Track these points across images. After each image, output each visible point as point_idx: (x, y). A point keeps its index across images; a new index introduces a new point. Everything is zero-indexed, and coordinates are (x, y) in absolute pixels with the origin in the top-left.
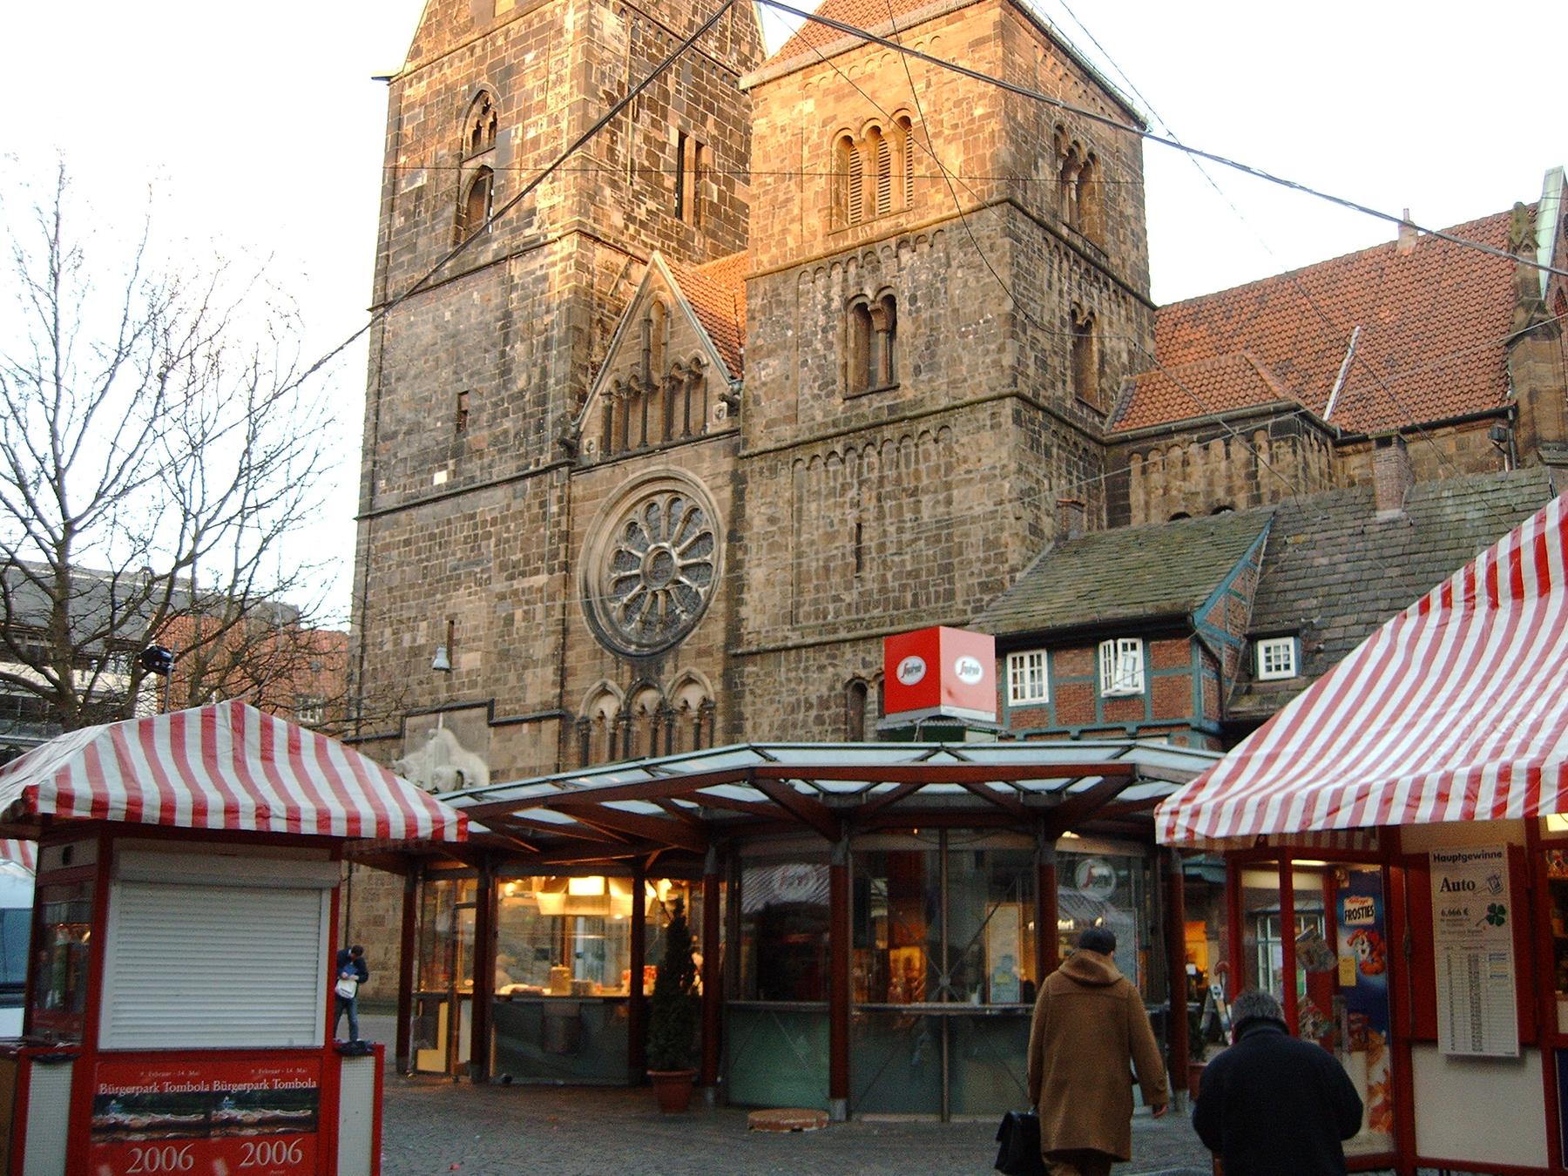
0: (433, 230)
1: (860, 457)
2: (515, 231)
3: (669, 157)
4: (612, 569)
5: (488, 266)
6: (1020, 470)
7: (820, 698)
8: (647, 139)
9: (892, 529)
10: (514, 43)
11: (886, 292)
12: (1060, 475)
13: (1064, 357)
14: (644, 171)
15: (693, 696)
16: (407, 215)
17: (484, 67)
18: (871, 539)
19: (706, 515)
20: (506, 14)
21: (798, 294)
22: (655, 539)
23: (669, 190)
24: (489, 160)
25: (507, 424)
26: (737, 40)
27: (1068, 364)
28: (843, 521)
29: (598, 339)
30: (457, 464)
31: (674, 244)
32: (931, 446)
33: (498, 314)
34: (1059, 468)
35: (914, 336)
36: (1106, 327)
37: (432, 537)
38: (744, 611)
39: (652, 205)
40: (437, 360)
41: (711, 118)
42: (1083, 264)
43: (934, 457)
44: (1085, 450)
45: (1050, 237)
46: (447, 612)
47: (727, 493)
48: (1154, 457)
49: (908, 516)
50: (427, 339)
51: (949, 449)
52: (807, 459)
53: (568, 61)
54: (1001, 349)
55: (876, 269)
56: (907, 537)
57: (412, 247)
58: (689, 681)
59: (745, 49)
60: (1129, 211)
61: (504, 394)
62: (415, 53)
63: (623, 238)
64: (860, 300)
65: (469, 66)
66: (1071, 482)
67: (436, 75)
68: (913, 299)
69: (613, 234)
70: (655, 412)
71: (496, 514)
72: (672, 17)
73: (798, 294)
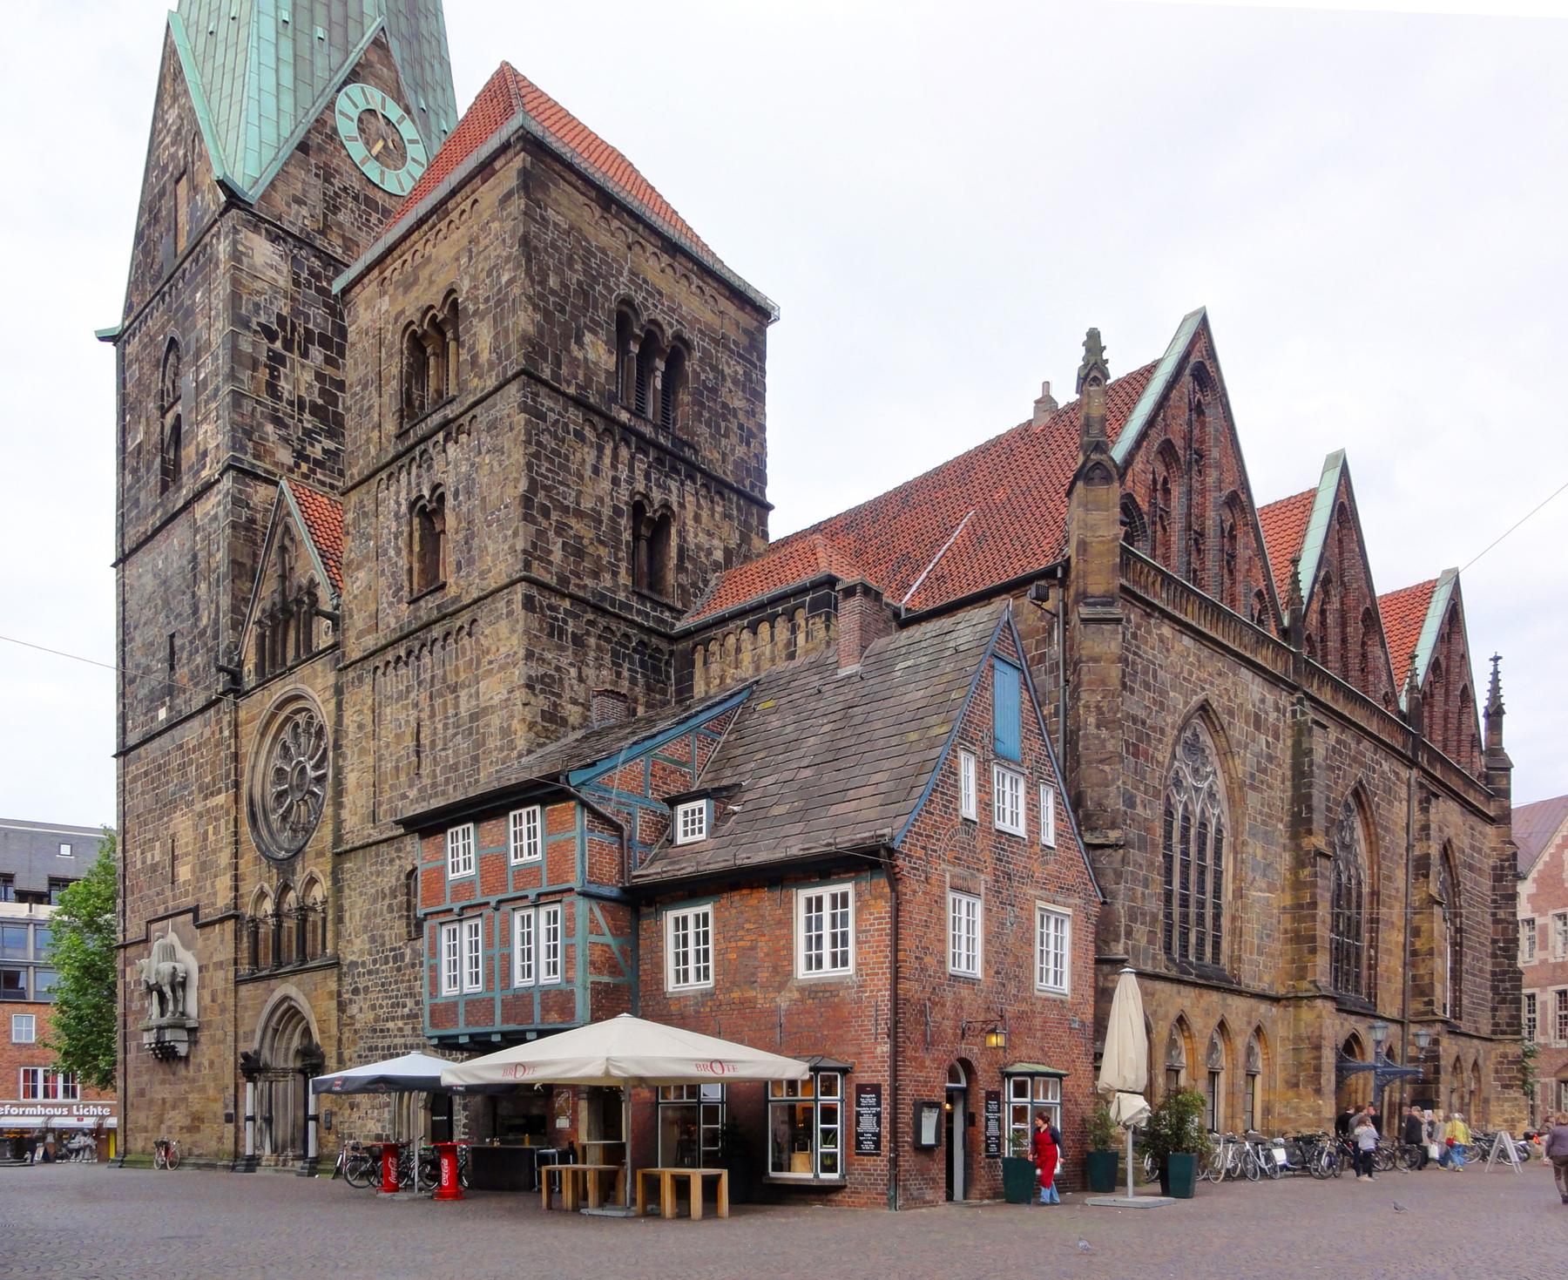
4: (274, 784)
6: (529, 655)
9: (440, 726)
13: (617, 548)
28: (407, 722)
42: (652, 454)
49: (451, 712)
51: (478, 641)
54: (515, 534)
56: (451, 731)
60: (738, 403)
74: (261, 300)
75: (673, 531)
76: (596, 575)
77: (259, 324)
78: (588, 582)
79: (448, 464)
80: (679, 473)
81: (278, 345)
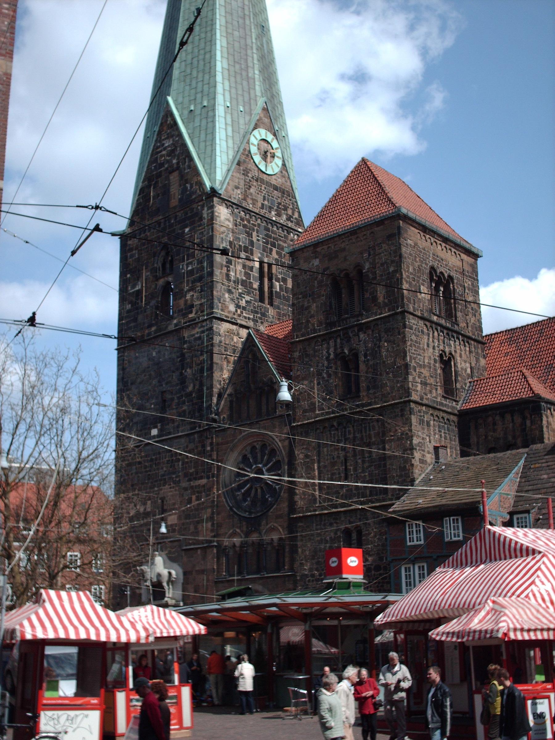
0: (145, 312)
1: (345, 428)
2: (185, 315)
3: (255, 273)
5: (172, 331)
7: (331, 538)
8: (244, 266)
9: (360, 461)
11: (354, 352)
12: (435, 434)
14: (244, 283)
15: (275, 537)
16: (131, 302)
18: (351, 465)
20: (175, 207)
21: (315, 351)
22: (256, 463)
23: (255, 289)
24: (170, 279)
25: (185, 408)
26: (286, 209)
27: (438, 380)
28: (338, 457)
29: (225, 366)
30: (162, 426)
31: (259, 315)
33: (178, 354)
34: (434, 430)
35: (367, 373)
36: (459, 358)
37: (152, 460)
38: (297, 498)
39: (248, 298)
40: (150, 375)
41: (274, 250)
42: (445, 331)
43: (377, 428)
44: (448, 420)
45: (427, 323)
46: (160, 496)
47: (286, 443)
51: (383, 424)
52: (321, 428)
53: (205, 233)
55: (349, 340)
56: (367, 464)
57: (135, 320)
58: (273, 529)
59: (290, 212)
61: (183, 393)
62: (132, 223)
63: (235, 317)
66: (441, 435)
68: (365, 356)
69: (230, 315)
72: (254, 204)
73: (315, 351)
74: (223, 236)
75: (453, 363)
76: (431, 392)
78: (429, 396)
79: (360, 341)
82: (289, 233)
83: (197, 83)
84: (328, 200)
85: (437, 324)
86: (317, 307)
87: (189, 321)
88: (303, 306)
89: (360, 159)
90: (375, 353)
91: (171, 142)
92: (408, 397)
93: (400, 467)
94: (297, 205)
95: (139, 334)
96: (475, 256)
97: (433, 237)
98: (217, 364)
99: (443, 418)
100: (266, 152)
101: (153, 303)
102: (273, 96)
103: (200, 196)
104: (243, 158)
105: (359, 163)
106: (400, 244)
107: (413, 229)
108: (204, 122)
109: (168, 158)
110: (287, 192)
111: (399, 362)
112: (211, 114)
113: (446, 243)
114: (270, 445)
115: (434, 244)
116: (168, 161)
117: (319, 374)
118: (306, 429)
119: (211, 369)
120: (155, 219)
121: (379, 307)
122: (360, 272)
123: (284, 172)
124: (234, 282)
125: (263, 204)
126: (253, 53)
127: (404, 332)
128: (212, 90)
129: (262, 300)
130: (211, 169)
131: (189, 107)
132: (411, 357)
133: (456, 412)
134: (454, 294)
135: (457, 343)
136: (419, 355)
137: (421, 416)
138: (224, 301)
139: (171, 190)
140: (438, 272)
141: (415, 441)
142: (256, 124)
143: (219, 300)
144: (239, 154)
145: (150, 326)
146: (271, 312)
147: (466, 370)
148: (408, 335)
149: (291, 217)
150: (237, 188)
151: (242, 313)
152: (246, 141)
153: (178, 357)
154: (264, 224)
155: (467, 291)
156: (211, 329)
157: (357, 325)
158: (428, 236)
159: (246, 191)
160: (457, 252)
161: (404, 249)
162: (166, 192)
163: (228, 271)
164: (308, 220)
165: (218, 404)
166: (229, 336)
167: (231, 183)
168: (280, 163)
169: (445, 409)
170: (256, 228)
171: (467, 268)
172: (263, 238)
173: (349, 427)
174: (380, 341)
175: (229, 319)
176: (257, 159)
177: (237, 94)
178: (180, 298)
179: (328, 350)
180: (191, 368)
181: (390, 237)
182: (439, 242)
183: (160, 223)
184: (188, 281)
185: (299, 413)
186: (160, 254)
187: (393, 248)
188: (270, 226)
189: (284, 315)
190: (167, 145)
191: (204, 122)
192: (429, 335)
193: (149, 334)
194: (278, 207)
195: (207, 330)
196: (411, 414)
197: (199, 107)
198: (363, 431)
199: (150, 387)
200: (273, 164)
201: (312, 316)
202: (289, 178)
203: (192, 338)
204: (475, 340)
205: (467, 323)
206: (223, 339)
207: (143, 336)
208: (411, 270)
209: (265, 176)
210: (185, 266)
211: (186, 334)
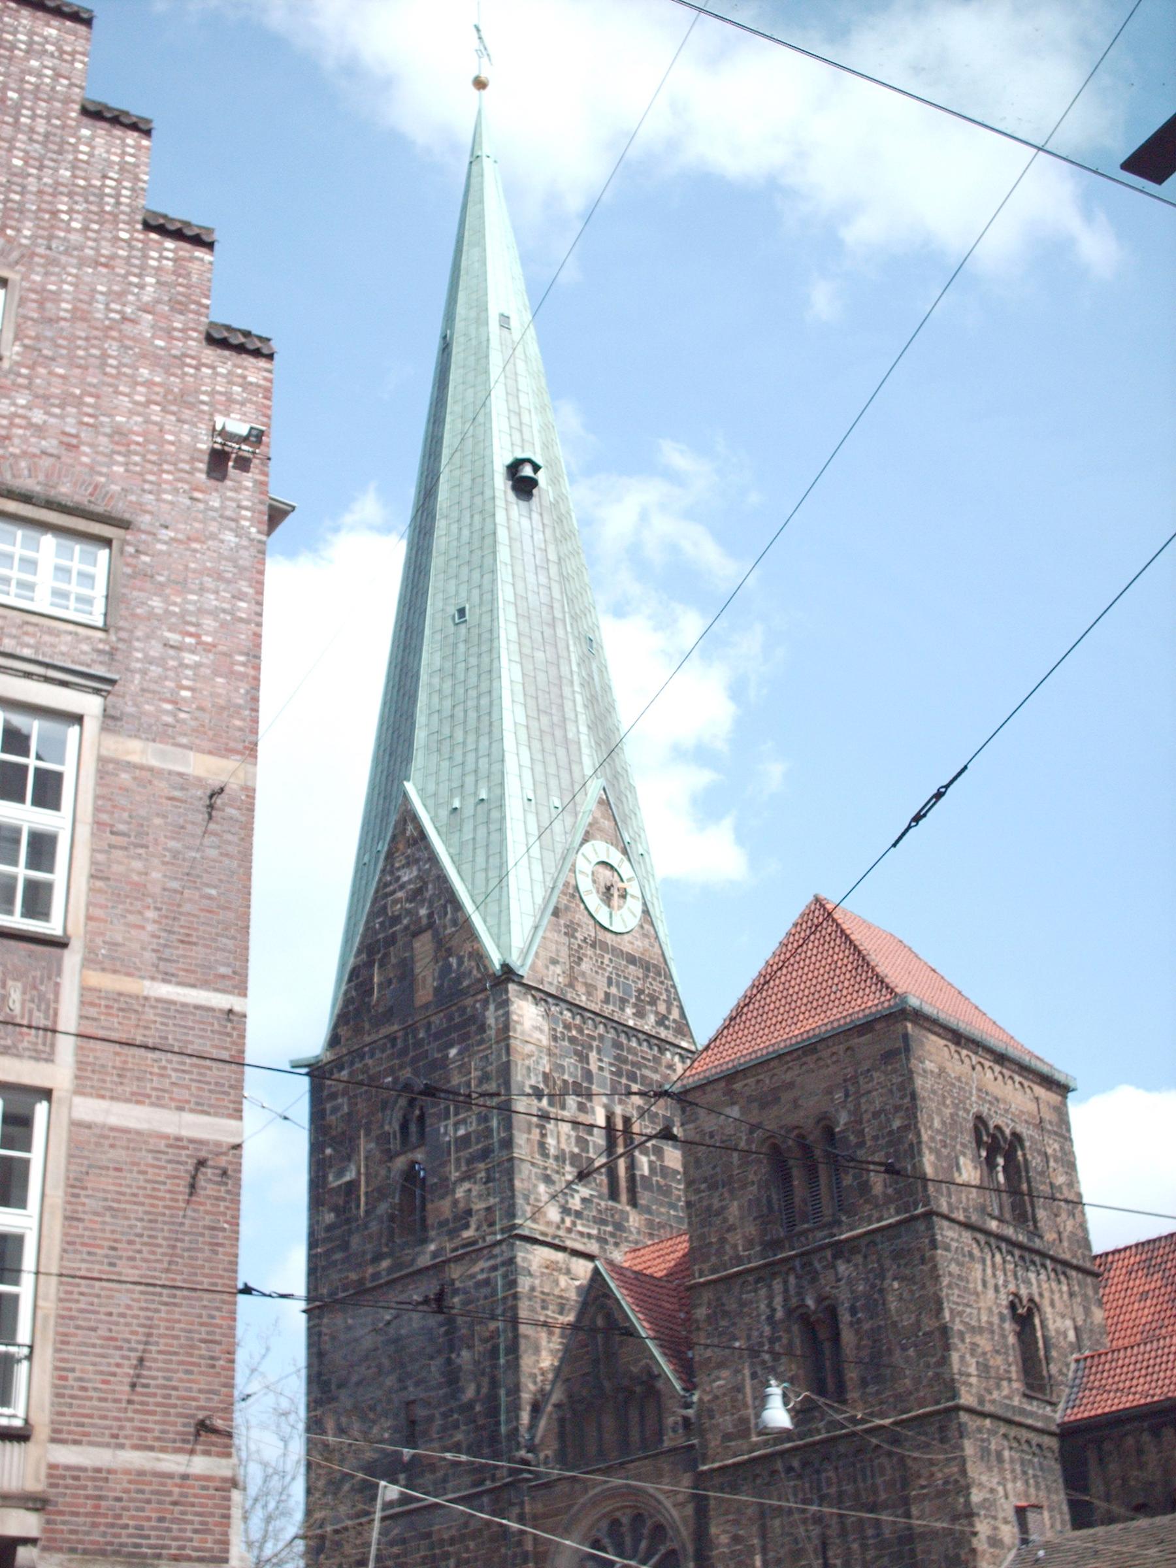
0: (366, 1228)
1: (818, 1472)
2: (453, 1233)
5: (427, 1268)
9: (855, 1546)
10: (437, 1036)
11: (826, 1303)
13: (1006, 1353)
16: (335, 1209)
17: (408, 1059)
18: (836, 1557)
19: (671, 1533)
20: (426, 1006)
21: (743, 1304)
24: (419, 1156)
26: (653, 1001)
27: (1011, 1359)
29: (544, 1343)
31: (609, 1229)
32: (884, 1460)
34: (1013, 1471)
35: (858, 1347)
36: (1048, 1310)
40: (379, 1366)
42: (1017, 1252)
43: (889, 1472)
44: (1039, 1446)
45: (980, 1236)
47: (689, 1510)
48: (1108, 1446)
49: (870, 1532)
50: (368, 1343)
55: (814, 1280)
56: (871, 1554)
57: (345, 1246)
59: (662, 1008)
60: (1060, 1180)
61: (454, 1404)
62: (334, 1040)
63: (561, 1233)
64: (800, 1311)
65: (391, 1057)
67: (358, 1065)
68: (853, 1311)
69: (551, 1231)
70: (609, 1422)
71: (453, 1532)
72: (589, 994)
75: (1037, 1321)
76: (998, 1387)
77: (532, 1087)
78: (995, 1395)
79: (839, 1280)
80: (1033, 1263)
81: (545, 1101)
82: (662, 1051)
83: (464, 754)
84: (749, 983)
85: (1000, 1238)
86: (741, 1207)
87: (464, 1246)
88: (709, 1208)
89: (811, 898)
90: (874, 1303)
91: (415, 873)
92: (953, 1398)
93: (946, 1557)
94: (676, 993)
95: (353, 1276)
96: (1062, 1089)
97: (976, 1053)
98: (527, 1337)
99: (1028, 1442)
100: (608, 889)
101: (383, 1208)
102: (616, 776)
103: (479, 980)
104: (565, 900)
105: (808, 907)
106: (911, 1072)
107: (933, 1038)
108: (482, 831)
109: (408, 906)
110: (655, 966)
111: (929, 1324)
112: (495, 814)
113: (1002, 1065)
114: (651, 1516)
115: (978, 1067)
116: (409, 912)
117: (754, 1352)
118: (733, 1476)
119: (514, 1349)
120: (385, 1031)
121: (877, 1206)
122: (829, 1134)
123: (646, 926)
124: (557, 1158)
125: (607, 995)
126: (574, 692)
127: (933, 1258)
128: (496, 767)
129: (614, 1195)
130: (499, 924)
131: (449, 802)
132: (952, 1311)
133: (1054, 1428)
134: (1027, 1172)
135: (1043, 1277)
136: (968, 1305)
137: (983, 1440)
138: (538, 1200)
139: (417, 971)
140: (991, 1125)
141: (976, 1496)
142: (587, 833)
143: (526, 1198)
144: (557, 892)
145: (378, 1258)
146: (634, 1220)
147: (1066, 1337)
148: (942, 1264)
149: (665, 1017)
150: (554, 962)
151: (574, 1224)
152: (568, 866)
153: (441, 1325)
154: (612, 1035)
155: (1052, 1164)
156: (511, 1261)
157: (830, 1245)
158: (964, 1052)
159: (572, 968)
160: (1026, 1083)
161: (919, 1081)
162: (406, 973)
163: (543, 1135)
164: (705, 1024)
165: (533, 1426)
166: (550, 1277)
167: (542, 953)
168: (638, 908)
169: (1029, 1421)
170: (595, 1044)
171: (1048, 1115)
172: (611, 1064)
173: (825, 1470)
174: (883, 1279)
175: (548, 1239)
176: (593, 901)
177: (546, 774)
178: (442, 1197)
179: (769, 1302)
180: (470, 1347)
181: (889, 1056)
182: (987, 1064)
183: (395, 1039)
184: (458, 1160)
185: (714, 1441)
186: (396, 1102)
187: (896, 1079)
188: (623, 1039)
189: (661, 1226)
190: (405, 879)
191: (482, 831)
192: (983, 1261)
193: (376, 1276)
194: (638, 998)
195: (504, 1264)
196: (961, 1437)
197: (471, 801)
198: (859, 1477)
199: (379, 1393)
200: (624, 910)
201: (731, 1229)
202: (657, 937)
203: (471, 1283)
204: (1078, 1269)
205: (1059, 1233)
206: (537, 1282)
207: (361, 1281)
208: (937, 1124)
209: (609, 935)
210: (451, 1129)
211: (455, 1272)
